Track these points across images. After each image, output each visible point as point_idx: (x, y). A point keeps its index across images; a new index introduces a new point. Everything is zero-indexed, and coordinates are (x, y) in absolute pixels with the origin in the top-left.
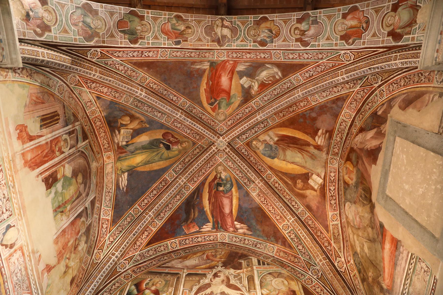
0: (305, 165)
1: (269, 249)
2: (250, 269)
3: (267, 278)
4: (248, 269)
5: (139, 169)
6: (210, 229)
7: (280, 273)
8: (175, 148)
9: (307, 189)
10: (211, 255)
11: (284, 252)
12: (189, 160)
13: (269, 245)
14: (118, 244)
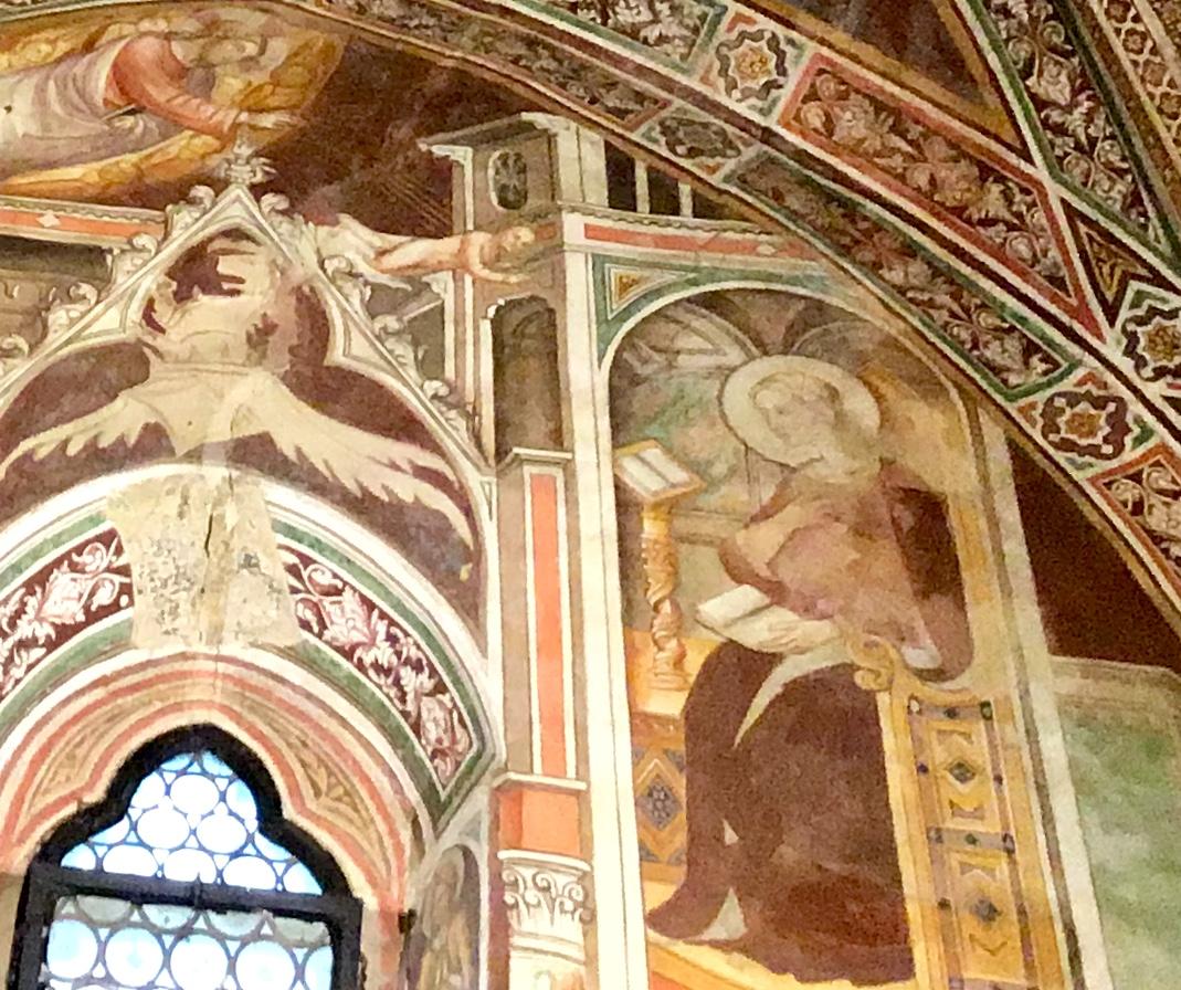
1: (732, 54)
2: (526, 235)
3: (680, 343)
4: (508, 239)
7: (818, 311)
10: (160, 63)
11: (879, 106)
13: (739, 18)
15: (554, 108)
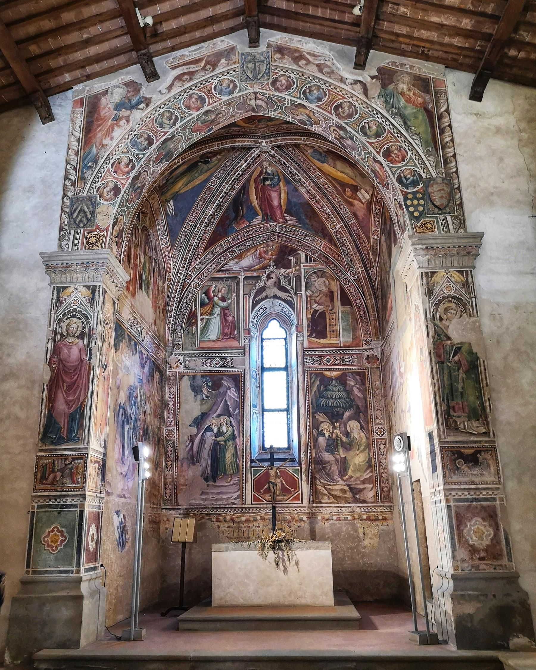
0: (354, 178)
5: (182, 191)
6: (260, 222)
8: (214, 159)
9: (355, 199)
11: (330, 248)
12: (231, 163)
14: (181, 262)
15: (300, 250)
